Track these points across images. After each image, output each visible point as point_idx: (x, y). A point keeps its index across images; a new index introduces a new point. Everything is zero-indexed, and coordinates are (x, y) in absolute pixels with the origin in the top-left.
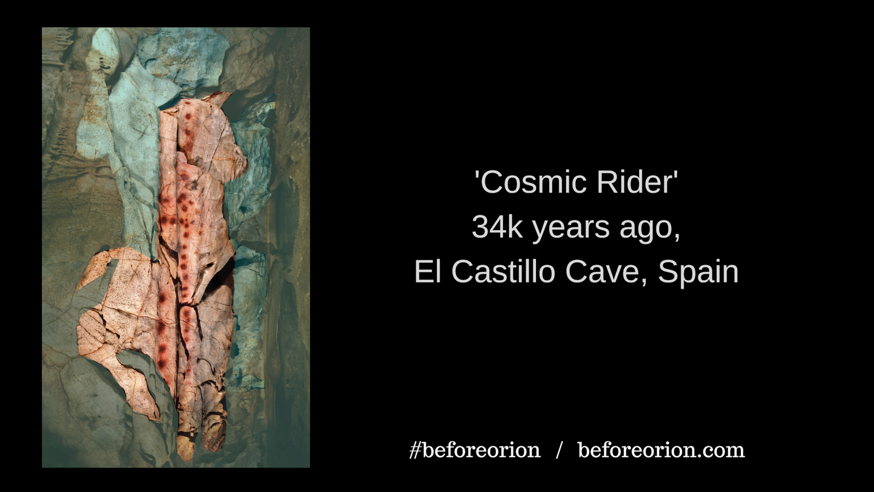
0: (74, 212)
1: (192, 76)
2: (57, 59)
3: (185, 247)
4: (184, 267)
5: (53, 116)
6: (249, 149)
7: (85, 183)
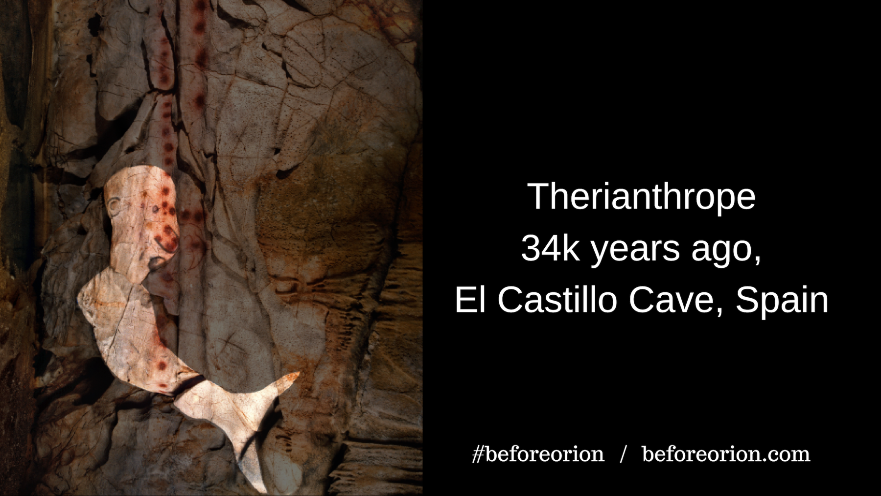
0: (329, 227)
1: (156, 425)
2: (353, 450)
4: (169, 147)
5: (359, 367)
6: (74, 318)
7: (312, 268)
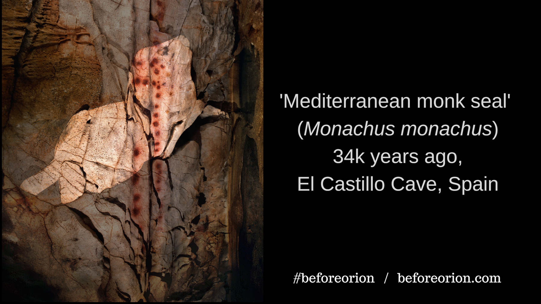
3: (157, 106)
4: (156, 124)
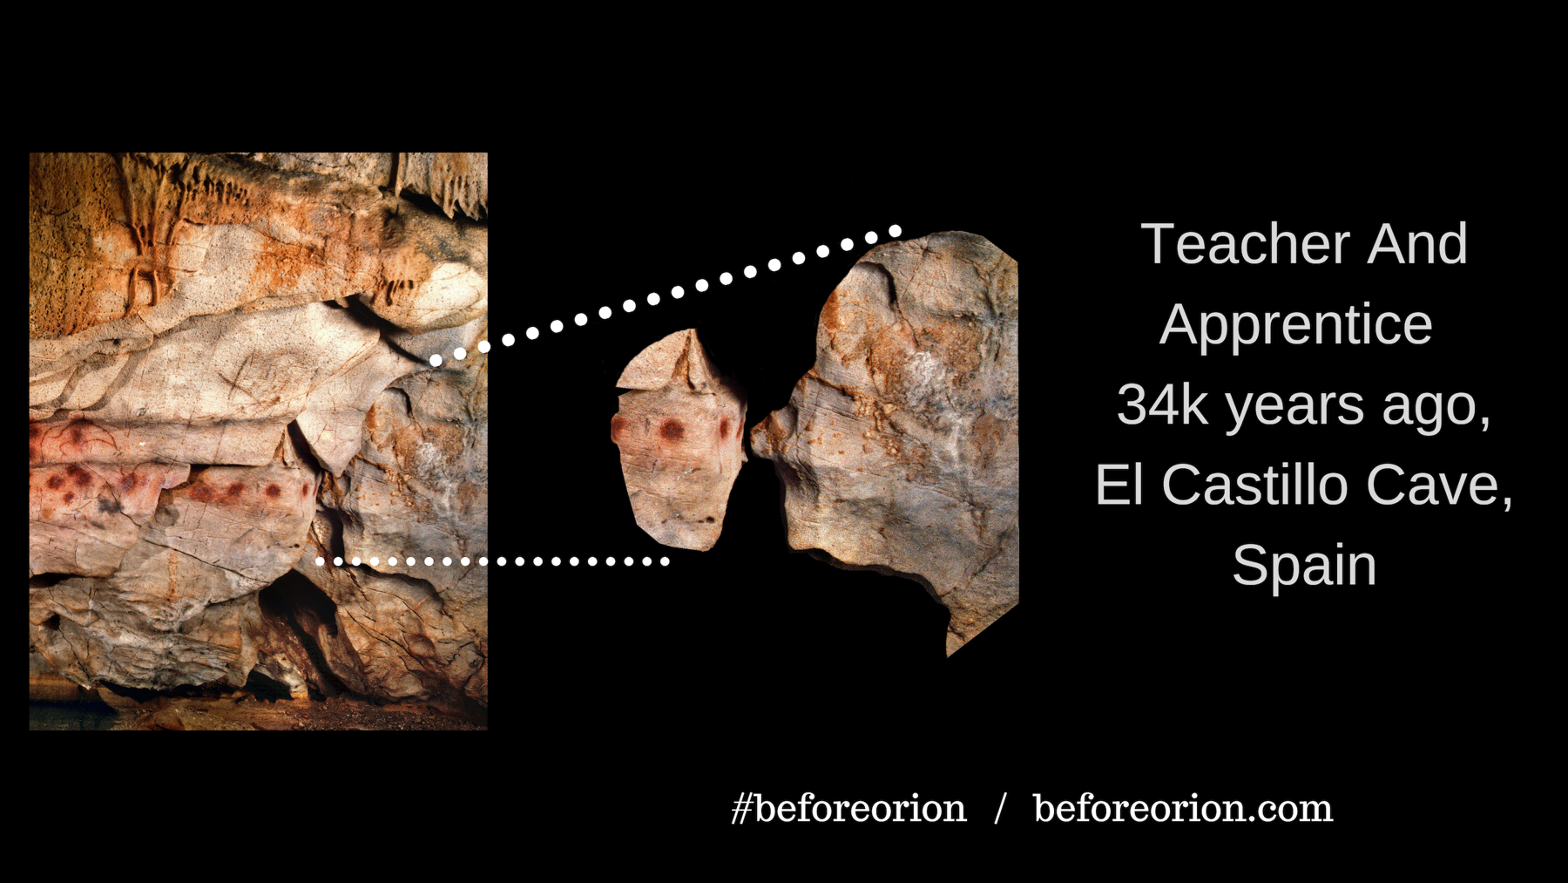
0: (47, 219)
1: (370, 501)
2: (411, 180)
5: (275, 169)
6: (196, 636)
7: (114, 247)
